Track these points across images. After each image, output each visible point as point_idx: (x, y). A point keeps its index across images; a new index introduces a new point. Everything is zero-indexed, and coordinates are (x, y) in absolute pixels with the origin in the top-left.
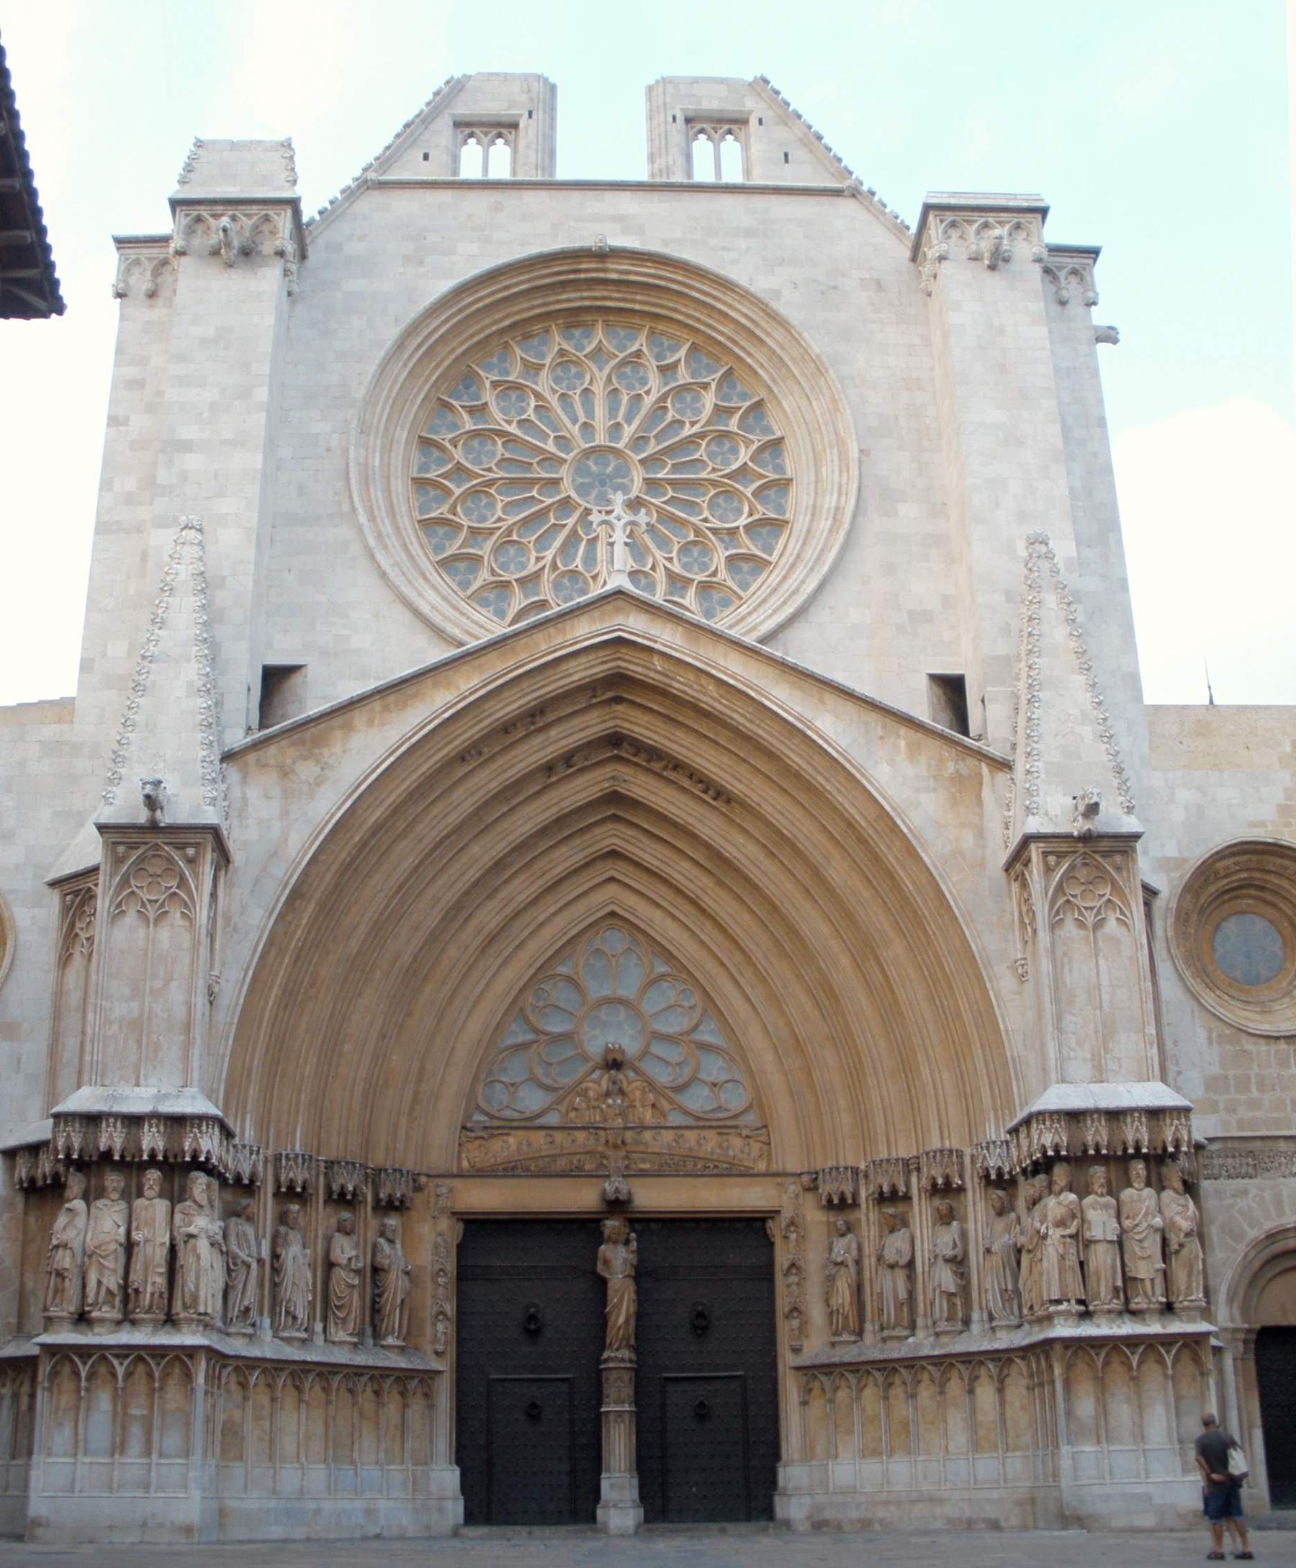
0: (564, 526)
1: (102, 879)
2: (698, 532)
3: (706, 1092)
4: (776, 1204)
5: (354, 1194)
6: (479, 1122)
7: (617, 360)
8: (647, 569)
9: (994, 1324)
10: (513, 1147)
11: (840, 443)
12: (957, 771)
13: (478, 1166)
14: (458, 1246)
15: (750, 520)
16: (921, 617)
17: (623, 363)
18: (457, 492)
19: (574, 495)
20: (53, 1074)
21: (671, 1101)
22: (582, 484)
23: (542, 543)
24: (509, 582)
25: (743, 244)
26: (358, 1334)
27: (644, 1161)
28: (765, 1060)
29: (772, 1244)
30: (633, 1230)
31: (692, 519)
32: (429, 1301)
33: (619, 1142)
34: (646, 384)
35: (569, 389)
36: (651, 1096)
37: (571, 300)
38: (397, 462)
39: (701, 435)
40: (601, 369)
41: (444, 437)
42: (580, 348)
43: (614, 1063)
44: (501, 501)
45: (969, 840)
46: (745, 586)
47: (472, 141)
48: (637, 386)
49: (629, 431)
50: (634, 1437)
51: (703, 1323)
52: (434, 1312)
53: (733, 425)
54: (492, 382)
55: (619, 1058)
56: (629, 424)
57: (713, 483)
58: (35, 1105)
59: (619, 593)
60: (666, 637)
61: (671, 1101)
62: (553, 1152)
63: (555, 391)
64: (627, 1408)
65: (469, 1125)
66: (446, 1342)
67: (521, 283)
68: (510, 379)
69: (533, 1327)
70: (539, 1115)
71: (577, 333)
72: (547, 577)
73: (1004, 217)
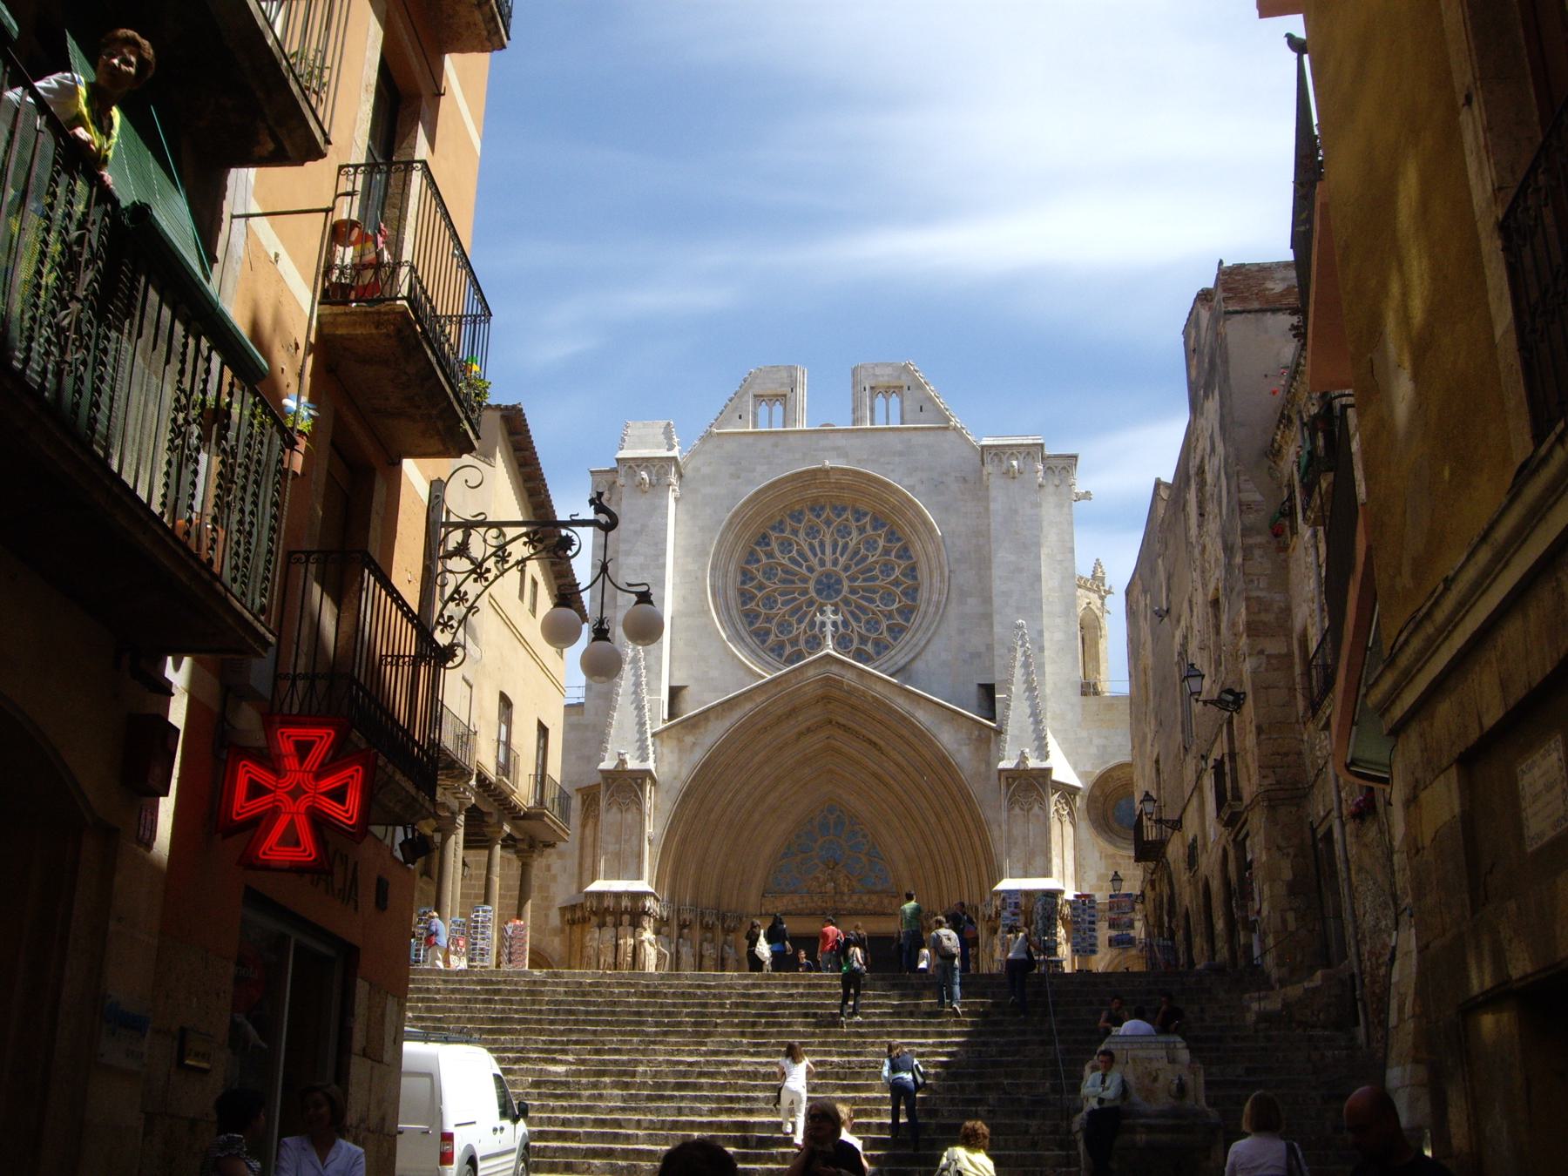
1: (603, 788)
2: (874, 613)
11: (941, 567)
12: (980, 735)
16: (976, 655)
17: (840, 524)
20: (581, 874)
23: (800, 621)
25: (897, 459)
36: (847, 882)
37: (813, 492)
38: (730, 582)
40: (829, 527)
42: (818, 516)
44: (780, 599)
45: (983, 766)
46: (895, 639)
47: (764, 403)
49: (842, 561)
57: (883, 588)
58: (574, 889)
59: (828, 655)
60: (849, 678)
67: (789, 487)
73: (1022, 449)
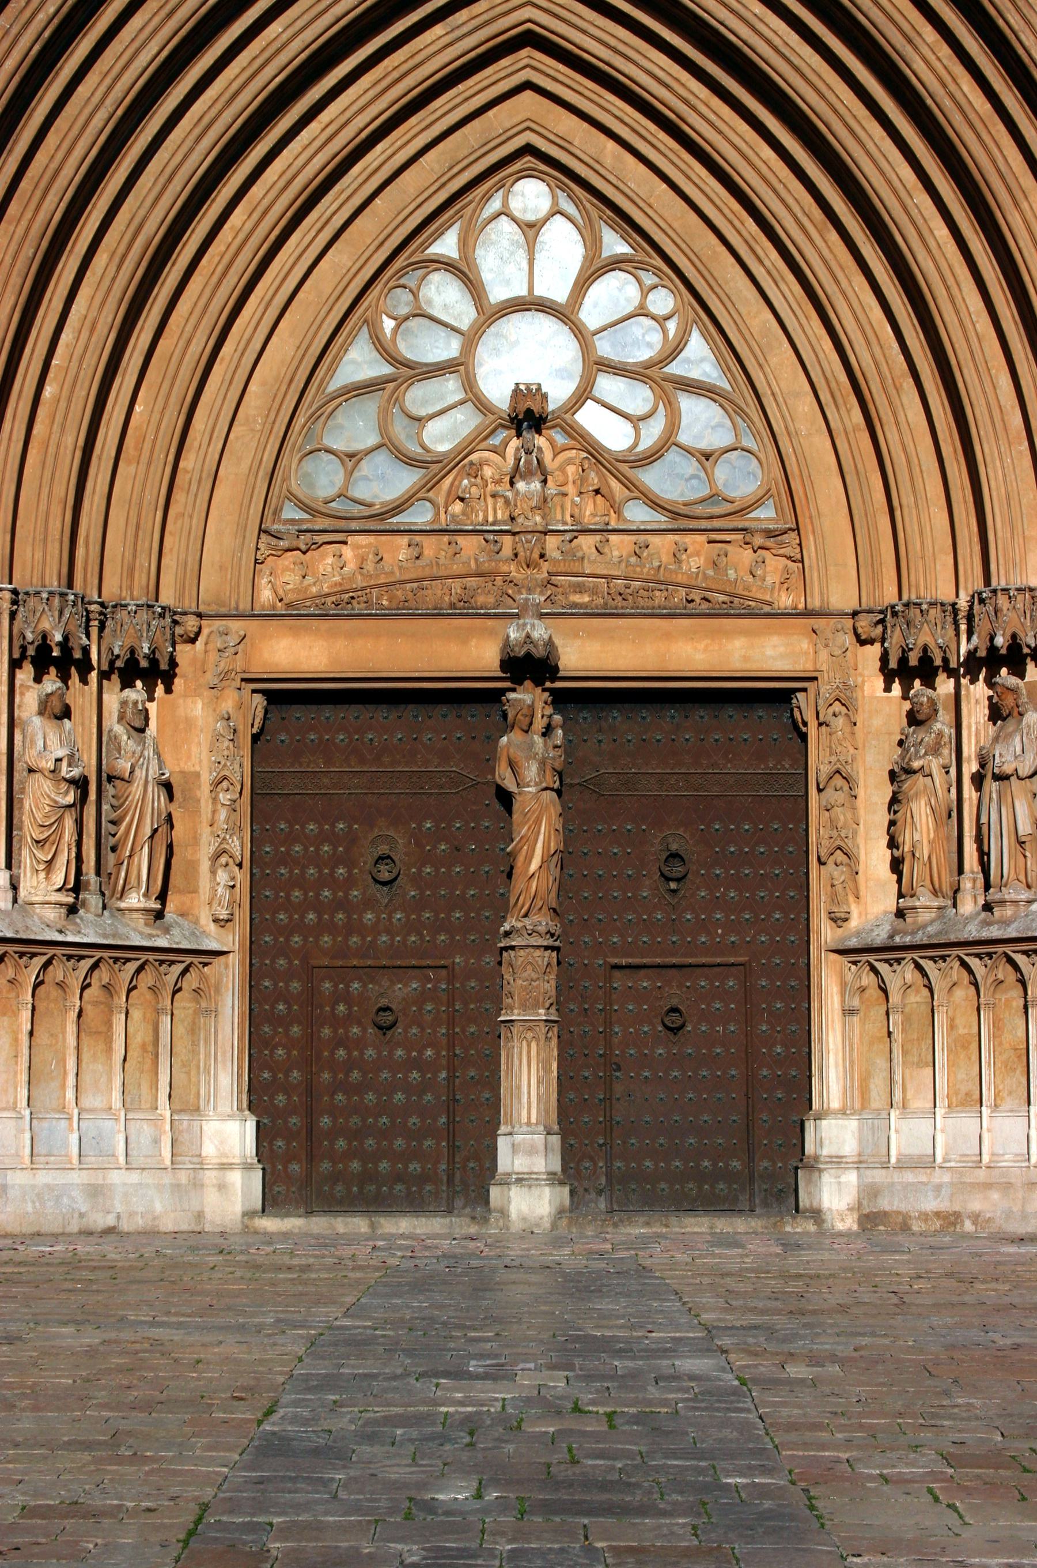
3: (691, 467)
4: (810, 666)
6: (293, 521)
10: (351, 567)
13: (290, 597)
14: (255, 738)
21: (629, 484)
27: (580, 589)
29: (804, 737)
32: (205, 832)
33: (536, 555)
50: (555, 1066)
51: (678, 870)
55: (536, 409)
61: (629, 484)
62: (420, 574)
64: (542, 1014)
66: (231, 903)
69: (386, 876)
70: (399, 507)
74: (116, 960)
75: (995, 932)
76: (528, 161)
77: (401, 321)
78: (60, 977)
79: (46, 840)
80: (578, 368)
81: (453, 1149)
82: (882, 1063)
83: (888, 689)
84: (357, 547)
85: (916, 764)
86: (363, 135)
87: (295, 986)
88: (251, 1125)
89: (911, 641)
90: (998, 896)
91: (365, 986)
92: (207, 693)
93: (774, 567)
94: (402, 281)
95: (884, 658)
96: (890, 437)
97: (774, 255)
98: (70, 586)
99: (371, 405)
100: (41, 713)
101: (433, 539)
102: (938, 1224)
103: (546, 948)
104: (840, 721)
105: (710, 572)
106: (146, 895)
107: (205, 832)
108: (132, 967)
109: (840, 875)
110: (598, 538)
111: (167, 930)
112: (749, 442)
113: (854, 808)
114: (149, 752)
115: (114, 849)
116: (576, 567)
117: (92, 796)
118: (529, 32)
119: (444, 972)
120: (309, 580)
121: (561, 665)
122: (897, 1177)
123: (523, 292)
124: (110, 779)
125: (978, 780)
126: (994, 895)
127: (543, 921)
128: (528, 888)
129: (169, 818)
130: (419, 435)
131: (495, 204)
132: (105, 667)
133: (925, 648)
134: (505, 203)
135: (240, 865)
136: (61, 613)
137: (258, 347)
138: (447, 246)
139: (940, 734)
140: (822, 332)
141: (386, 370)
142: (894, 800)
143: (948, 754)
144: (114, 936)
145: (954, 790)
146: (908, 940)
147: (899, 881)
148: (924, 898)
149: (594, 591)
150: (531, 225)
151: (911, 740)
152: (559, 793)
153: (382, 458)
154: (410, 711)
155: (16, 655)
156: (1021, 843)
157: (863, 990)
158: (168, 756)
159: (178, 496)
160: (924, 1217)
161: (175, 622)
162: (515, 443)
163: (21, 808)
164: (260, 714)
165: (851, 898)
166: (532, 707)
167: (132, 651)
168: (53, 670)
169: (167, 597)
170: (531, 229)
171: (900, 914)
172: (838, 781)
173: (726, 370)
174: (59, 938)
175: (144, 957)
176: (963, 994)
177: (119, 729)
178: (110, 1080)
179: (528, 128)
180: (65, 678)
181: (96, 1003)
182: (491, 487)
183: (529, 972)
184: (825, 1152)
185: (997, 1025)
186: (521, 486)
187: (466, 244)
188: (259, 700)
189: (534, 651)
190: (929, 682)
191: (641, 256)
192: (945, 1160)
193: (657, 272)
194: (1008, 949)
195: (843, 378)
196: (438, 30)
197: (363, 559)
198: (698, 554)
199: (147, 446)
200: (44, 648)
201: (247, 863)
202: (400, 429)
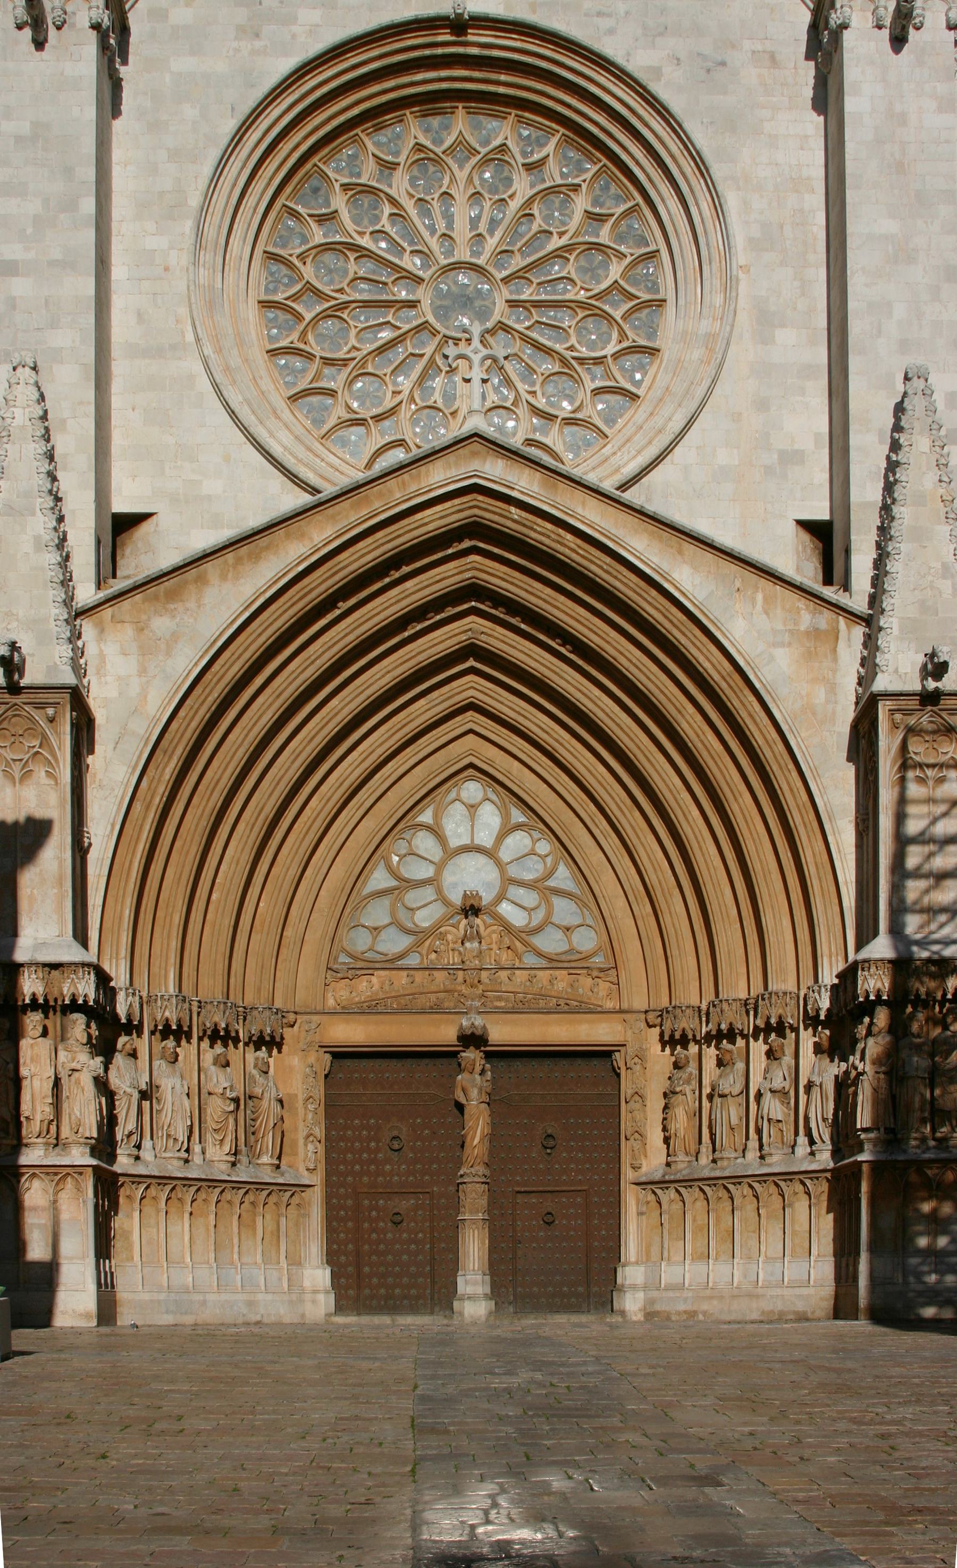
0: (422, 355)
2: (564, 361)
3: (559, 935)
5: (227, 1030)
6: (344, 963)
7: (479, 157)
8: (508, 404)
9: (814, 1148)
15: (618, 348)
18: (308, 316)
19: (432, 320)
21: (525, 944)
22: (440, 307)
24: (365, 420)
26: (235, 1154)
28: (616, 906)
30: (488, 1062)
31: (558, 347)
32: (301, 1125)
33: (476, 981)
34: (510, 186)
35: (426, 194)
39: (569, 248)
40: (461, 167)
41: (292, 251)
42: (438, 141)
43: (471, 909)
48: (501, 188)
49: (491, 242)
52: (305, 1133)
53: (604, 235)
54: (342, 185)
56: (492, 236)
61: (525, 944)
62: (414, 991)
63: (413, 197)
65: (335, 966)
68: (362, 181)
70: (402, 956)
71: (435, 122)
72: (405, 413)
74: (257, 1189)
75: (718, 1174)
76: (471, 771)
77: (402, 857)
78: (229, 1198)
79: (219, 1129)
80: (498, 883)
81: (433, 1283)
82: (657, 1239)
83: (663, 1050)
84: (379, 977)
85: (678, 1089)
86: (382, 758)
87: (350, 1202)
88: (328, 1272)
89: (676, 1026)
90: (719, 1156)
91: (386, 1202)
92: (301, 1053)
93: (603, 987)
94: (402, 836)
95: (662, 1035)
96: (666, 920)
97: (604, 822)
98: (228, 998)
99: (386, 901)
100: (215, 1064)
101: (420, 972)
102: (685, 1317)
103: (483, 1183)
104: (638, 1067)
105: (569, 990)
106: (271, 1156)
107: (301, 1125)
108: (265, 1193)
109: (637, 1145)
110: (509, 972)
111: (282, 1175)
112: (590, 921)
113: (645, 1112)
114: (271, 1084)
115: (253, 1133)
116: (497, 988)
117: (242, 1107)
118: (472, 703)
119: (428, 1195)
120: (354, 994)
121: (489, 1039)
122: (665, 1294)
123: (469, 842)
124: (250, 1097)
125: (710, 1097)
126: (717, 1154)
127: (481, 1169)
128: (473, 1153)
129: (282, 1118)
130: (412, 918)
131: (453, 795)
132: (247, 1040)
133: (684, 1030)
134: (458, 794)
135: (320, 1142)
136: (224, 1013)
137: (325, 871)
138: (426, 817)
139: (691, 1074)
140: (630, 864)
141: (394, 883)
142: (666, 1107)
143: (695, 1084)
144: (256, 1177)
145: (697, 1102)
146: (672, 1178)
147: (668, 1148)
148: (681, 1157)
149: (507, 1000)
150: (472, 806)
151: (675, 1077)
152: (488, 1104)
153: (392, 930)
154: (409, 1062)
155: (201, 1034)
156: (732, 1129)
157: (648, 1203)
158: (280, 1086)
159: (283, 950)
160: (678, 1313)
161: (283, 1017)
162: (464, 922)
163: (205, 1112)
164: (329, 1064)
165: (642, 1157)
166: (474, 1060)
167: (261, 1032)
168: (219, 1042)
169: (278, 1004)
170: (472, 808)
171: (668, 1164)
172: (637, 1098)
173: (578, 884)
174: (229, 1179)
175: (272, 1188)
176: (701, 1204)
177: (255, 1072)
178: (256, 1249)
179: (471, 754)
180: (226, 1046)
181: (248, 1211)
182: (451, 945)
183: (474, 1194)
184: (627, 1282)
185: (718, 1220)
186: (468, 945)
187: (436, 816)
188: (328, 1057)
189: (476, 1032)
190: (685, 1047)
191: (532, 823)
192: (690, 1285)
193: (541, 832)
194: (724, 1182)
195: (641, 888)
196: (422, 702)
197: (383, 983)
198: (562, 980)
199: (267, 924)
200: (216, 1031)
201: (323, 1141)
202: (402, 915)
